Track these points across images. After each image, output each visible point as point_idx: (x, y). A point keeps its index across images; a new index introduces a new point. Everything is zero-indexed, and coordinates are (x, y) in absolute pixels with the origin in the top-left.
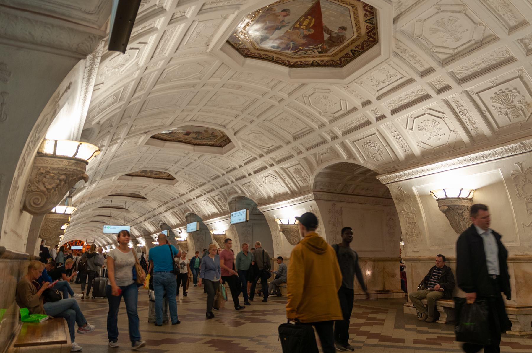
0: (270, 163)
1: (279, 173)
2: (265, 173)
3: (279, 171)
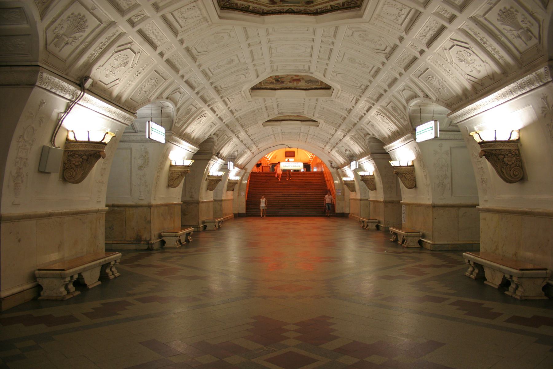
0: (447, 16)
1: (472, 33)
2: (444, 41)
3: (470, 29)
